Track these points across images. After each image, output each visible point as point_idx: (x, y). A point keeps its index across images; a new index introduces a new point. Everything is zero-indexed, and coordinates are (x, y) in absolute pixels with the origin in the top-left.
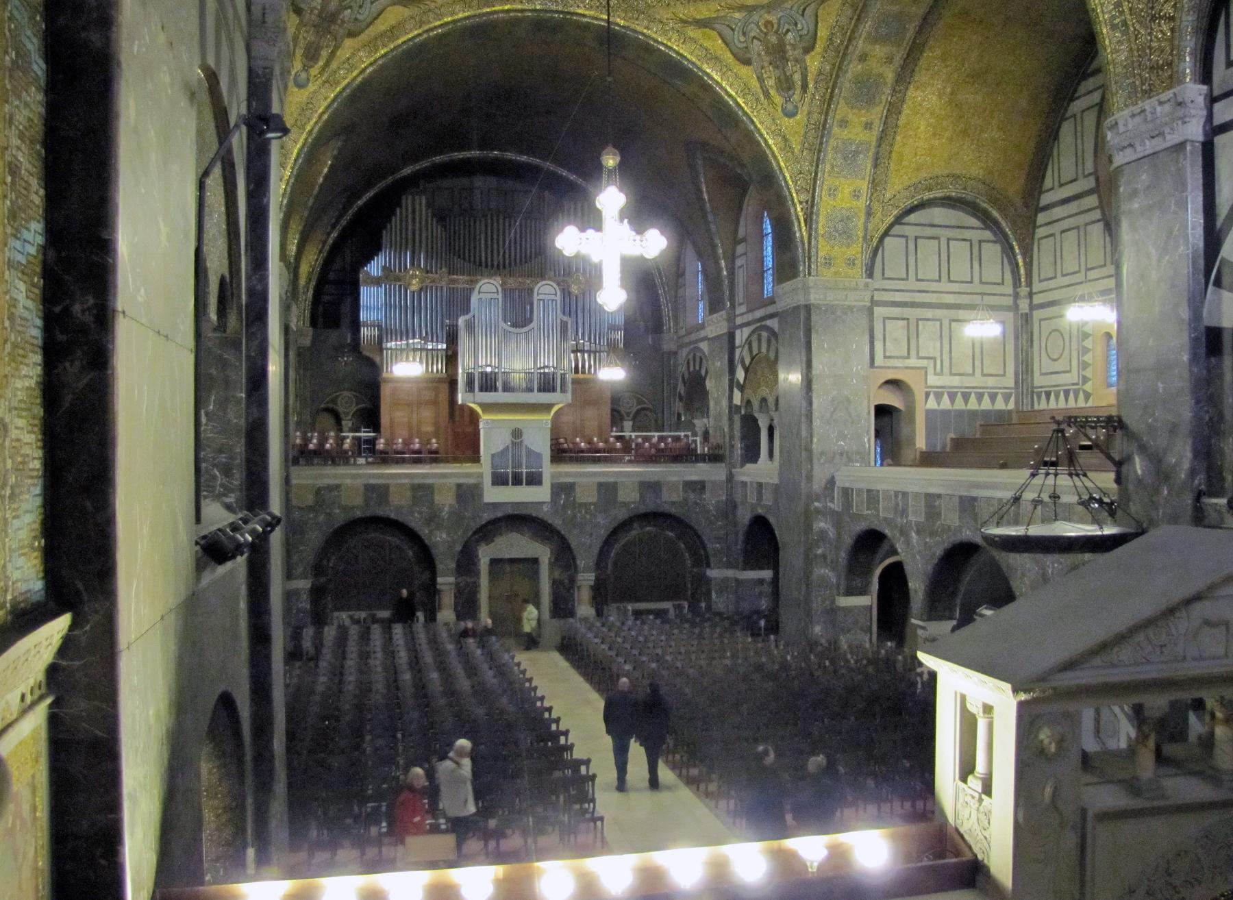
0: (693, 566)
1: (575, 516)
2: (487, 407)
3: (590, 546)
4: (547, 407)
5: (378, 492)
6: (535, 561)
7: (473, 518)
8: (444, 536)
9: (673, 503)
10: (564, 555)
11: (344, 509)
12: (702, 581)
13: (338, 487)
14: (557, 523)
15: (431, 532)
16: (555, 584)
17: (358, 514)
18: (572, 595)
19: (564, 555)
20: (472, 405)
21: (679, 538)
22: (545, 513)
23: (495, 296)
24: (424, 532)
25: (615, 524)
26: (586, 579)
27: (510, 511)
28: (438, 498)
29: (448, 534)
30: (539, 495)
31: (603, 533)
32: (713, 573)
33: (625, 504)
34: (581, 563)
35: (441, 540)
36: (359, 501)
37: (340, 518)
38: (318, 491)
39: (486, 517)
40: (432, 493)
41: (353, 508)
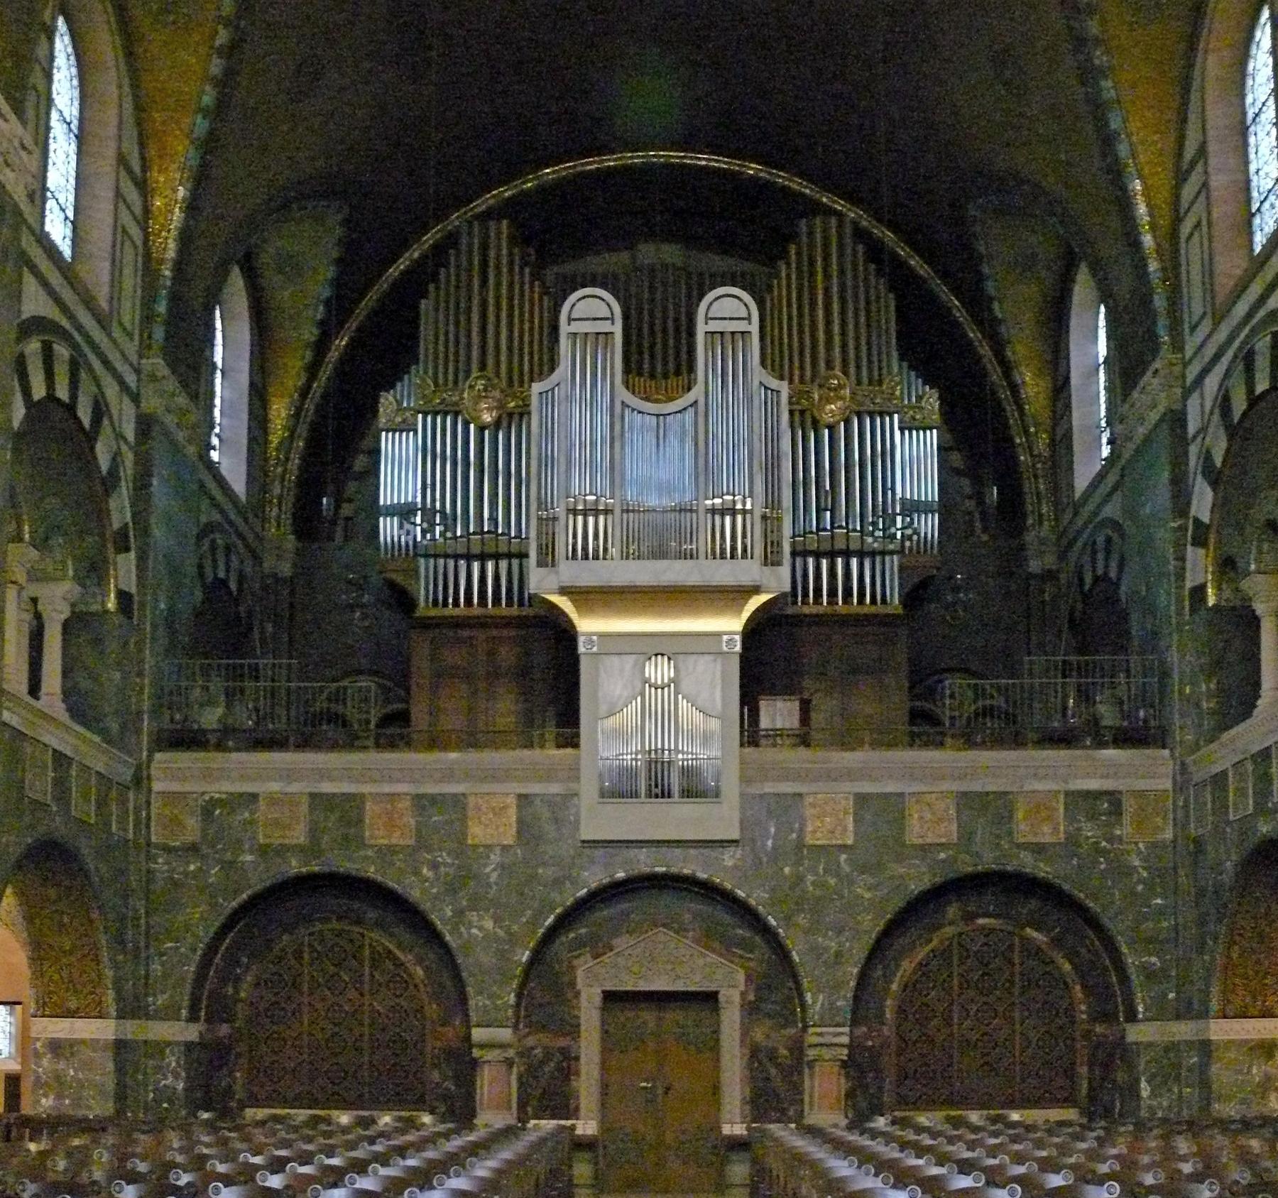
0: (1093, 1020)
1: (800, 879)
2: (587, 597)
3: (838, 954)
4: (735, 595)
5: (343, 812)
6: (710, 998)
7: (557, 883)
8: (489, 924)
9: (1039, 849)
10: (778, 982)
11: (263, 851)
12: (1113, 1057)
13: (254, 797)
14: (756, 897)
15: (459, 913)
16: (756, 1055)
17: (295, 866)
18: (797, 1089)
19: (778, 982)
20: (555, 599)
21: (1057, 942)
22: (723, 870)
23: (605, 327)
24: (441, 916)
25: (898, 903)
26: (830, 1039)
27: (646, 862)
28: (477, 832)
29: (497, 920)
30: (720, 820)
31: (871, 925)
32: (1137, 1033)
33: (925, 849)
34: (815, 1001)
35: (488, 939)
36: (299, 835)
37: (258, 880)
38: (207, 812)
39: (594, 878)
40: (464, 819)
41: (282, 851)
